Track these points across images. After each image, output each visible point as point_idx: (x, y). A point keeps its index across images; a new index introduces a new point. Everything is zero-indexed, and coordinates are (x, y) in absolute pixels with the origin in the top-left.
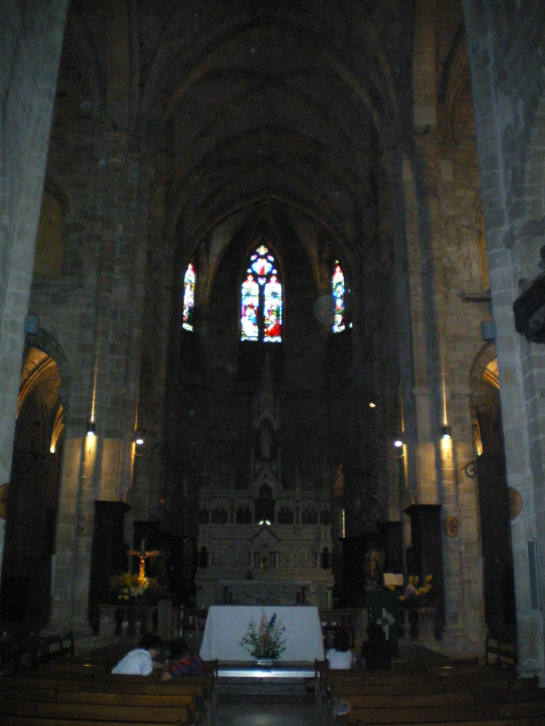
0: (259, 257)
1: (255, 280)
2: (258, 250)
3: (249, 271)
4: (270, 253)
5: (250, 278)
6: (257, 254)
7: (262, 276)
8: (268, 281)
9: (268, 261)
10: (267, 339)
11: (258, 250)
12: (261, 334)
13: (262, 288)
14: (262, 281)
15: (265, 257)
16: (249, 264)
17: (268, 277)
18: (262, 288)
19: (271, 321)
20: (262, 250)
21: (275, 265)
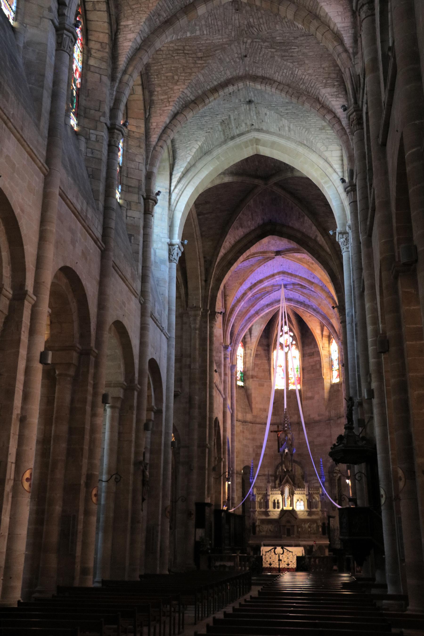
12: (287, 385)
13: (286, 354)
14: (286, 349)
18: (286, 354)
21: (294, 338)
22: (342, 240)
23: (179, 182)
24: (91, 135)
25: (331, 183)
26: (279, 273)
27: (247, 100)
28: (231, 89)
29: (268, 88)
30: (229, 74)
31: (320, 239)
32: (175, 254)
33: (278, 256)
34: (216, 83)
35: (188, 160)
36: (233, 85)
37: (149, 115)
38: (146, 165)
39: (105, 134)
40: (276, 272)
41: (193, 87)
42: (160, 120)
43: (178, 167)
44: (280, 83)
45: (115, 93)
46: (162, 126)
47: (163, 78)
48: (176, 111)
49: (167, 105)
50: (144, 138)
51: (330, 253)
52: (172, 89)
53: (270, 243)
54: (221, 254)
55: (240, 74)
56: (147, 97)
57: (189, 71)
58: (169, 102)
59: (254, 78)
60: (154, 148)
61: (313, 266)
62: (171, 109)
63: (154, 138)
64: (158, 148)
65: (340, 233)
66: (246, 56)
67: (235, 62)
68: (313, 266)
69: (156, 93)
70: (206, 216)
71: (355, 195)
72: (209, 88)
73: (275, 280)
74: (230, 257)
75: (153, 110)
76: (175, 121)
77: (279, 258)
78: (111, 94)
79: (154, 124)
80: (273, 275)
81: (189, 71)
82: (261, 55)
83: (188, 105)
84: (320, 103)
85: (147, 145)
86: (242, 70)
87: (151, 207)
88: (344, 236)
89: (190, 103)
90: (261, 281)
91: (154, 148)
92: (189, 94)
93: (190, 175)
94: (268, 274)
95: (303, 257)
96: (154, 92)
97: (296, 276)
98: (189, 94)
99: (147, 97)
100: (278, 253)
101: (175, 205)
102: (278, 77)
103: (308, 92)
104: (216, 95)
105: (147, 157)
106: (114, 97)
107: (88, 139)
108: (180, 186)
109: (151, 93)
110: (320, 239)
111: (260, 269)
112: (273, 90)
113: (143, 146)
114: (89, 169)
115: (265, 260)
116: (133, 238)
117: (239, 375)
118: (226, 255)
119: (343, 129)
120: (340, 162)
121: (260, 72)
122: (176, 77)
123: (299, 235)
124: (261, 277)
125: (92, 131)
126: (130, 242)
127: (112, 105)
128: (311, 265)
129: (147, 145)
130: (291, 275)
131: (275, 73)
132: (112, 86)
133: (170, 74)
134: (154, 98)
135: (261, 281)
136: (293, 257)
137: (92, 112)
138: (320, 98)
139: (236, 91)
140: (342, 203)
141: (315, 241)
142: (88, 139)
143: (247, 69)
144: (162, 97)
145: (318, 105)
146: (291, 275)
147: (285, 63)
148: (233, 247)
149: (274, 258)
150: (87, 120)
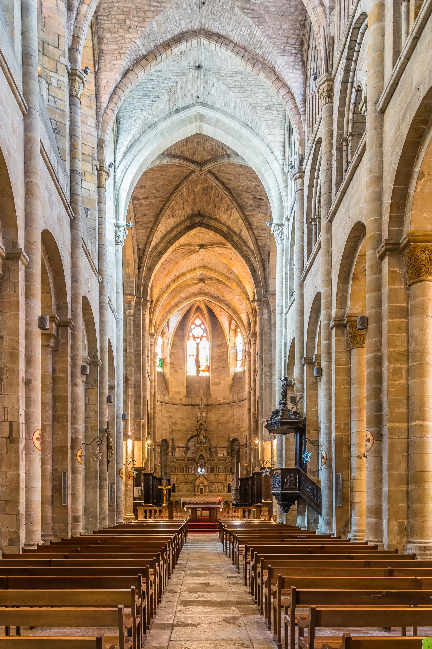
0: (196, 326)
1: (194, 339)
2: (195, 322)
3: (191, 334)
4: (203, 323)
5: (191, 338)
6: (195, 324)
7: (198, 338)
8: (201, 340)
9: (202, 328)
10: (201, 374)
11: (195, 322)
15: (200, 326)
16: (191, 330)
17: (201, 338)
19: (204, 363)
20: (198, 322)
22: (278, 232)
23: (123, 158)
24: (52, 79)
25: (271, 172)
26: (200, 267)
27: (197, 65)
28: (184, 46)
29: (223, 49)
30: (184, 27)
31: (245, 234)
32: (121, 236)
33: (201, 250)
34: (169, 36)
35: (133, 132)
36: (187, 41)
37: (98, 69)
38: (98, 130)
39: (65, 79)
40: (197, 266)
41: (145, 38)
42: (110, 76)
43: (123, 140)
44: (235, 44)
45: (72, 28)
46: (113, 84)
47: (114, 21)
48: (127, 68)
49: (118, 57)
50: (94, 97)
51: (253, 248)
52: (123, 37)
53: (198, 235)
54: (153, 243)
55: (195, 28)
56: (96, 46)
57: (142, 14)
58: (120, 54)
59: (210, 35)
60: (105, 111)
61: (231, 262)
62: (124, 63)
63: (104, 99)
64: (109, 112)
65: (276, 225)
66: (204, 3)
67: (192, 9)
68: (231, 262)
69: (105, 41)
70: (141, 201)
71: (303, 182)
72: (161, 41)
73: (195, 274)
74: (161, 247)
75: (102, 62)
76: (125, 80)
77: (202, 252)
78: (69, 28)
79: (105, 81)
80: (195, 269)
81: (142, 14)
82: (220, 4)
83: (142, 60)
84: (275, 75)
85: (98, 107)
86: (197, 23)
87: (104, 180)
88: (280, 227)
89: (142, 59)
90: (183, 274)
91: (105, 111)
92: (141, 47)
93: (134, 150)
94: (190, 268)
95: (223, 252)
96: (103, 39)
97: (215, 271)
98: (141, 47)
99: (96, 46)
100: (202, 246)
101: (120, 183)
102: (235, 37)
103: (264, 60)
104: (169, 52)
105: (98, 122)
106: (72, 34)
107: (49, 84)
108: (124, 162)
109: (100, 39)
110: (245, 234)
111: (183, 262)
112: (229, 52)
113: (94, 107)
114: (52, 121)
115: (189, 253)
116: (89, 212)
117: (158, 361)
118: (157, 245)
119: (296, 107)
120: (282, 149)
121: (215, 28)
122: (128, 22)
123: (225, 229)
124: (184, 269)
125: (52, 74)
126: (87, 216)
127: (70, 43)
128: (230, 261)
129: (98, 107)
130: (211, 269)
131: (232, 30)
132: (69, 18)
133: (121, 17)
134: (104, 47)
135: (183, 274)
136: (215, 251)
137: (51, 48)
138: (277, 68)
139: (188, 50)
140: (280, 194)
141: (240, 236)
142: (49, 84)
143: (203, 22)
144: (113, 47)
145: (273, 76)
146: (211, 269)
147: (245, 17)
148: (164, 237)
149: (198, 251)
150: (46, 58)
